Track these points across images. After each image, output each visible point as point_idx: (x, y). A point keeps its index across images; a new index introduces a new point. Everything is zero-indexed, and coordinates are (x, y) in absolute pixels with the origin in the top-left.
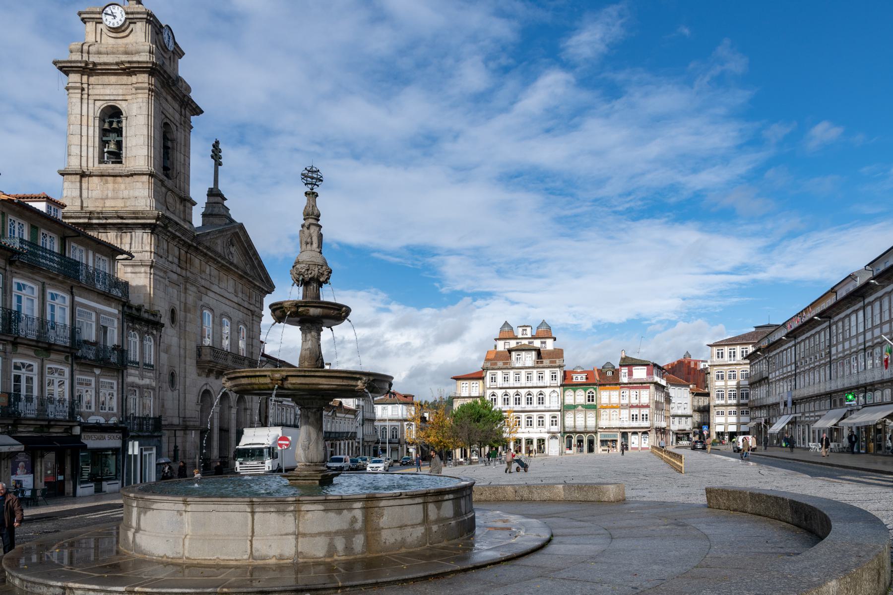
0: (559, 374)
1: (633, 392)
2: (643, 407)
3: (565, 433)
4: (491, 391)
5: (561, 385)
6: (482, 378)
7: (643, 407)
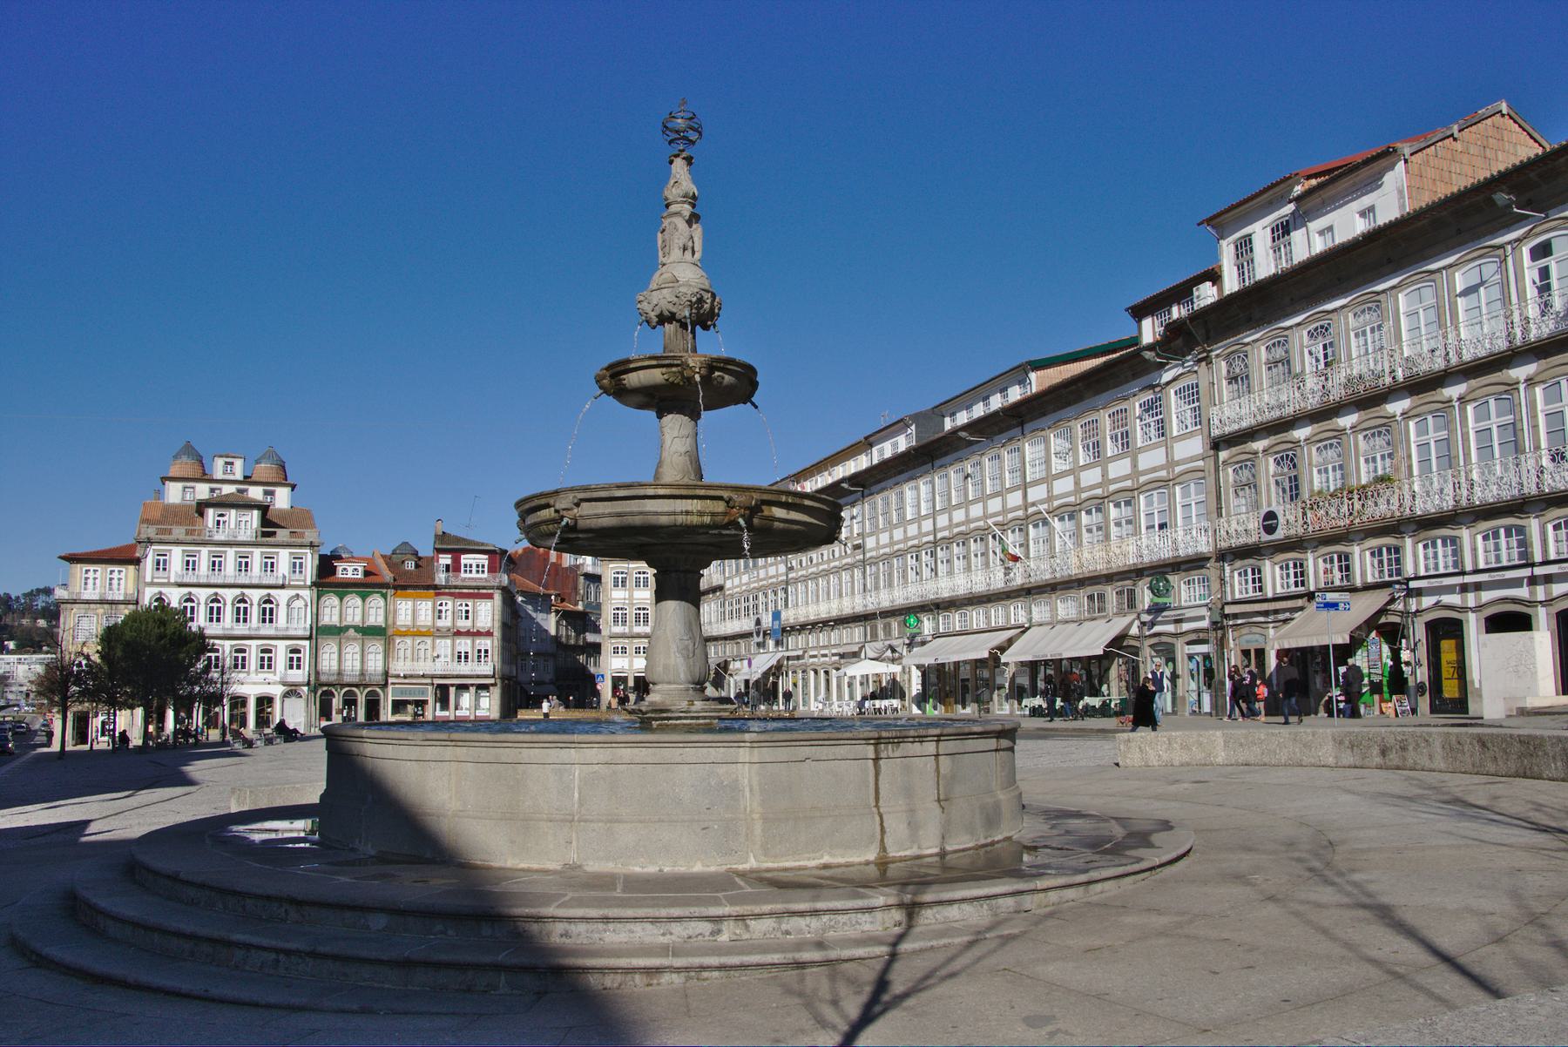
0: (310, 563)
2: (479, 634)
4: (156, 590)
5: (314, 584)
6: (137, 562)
7: (479, 634)
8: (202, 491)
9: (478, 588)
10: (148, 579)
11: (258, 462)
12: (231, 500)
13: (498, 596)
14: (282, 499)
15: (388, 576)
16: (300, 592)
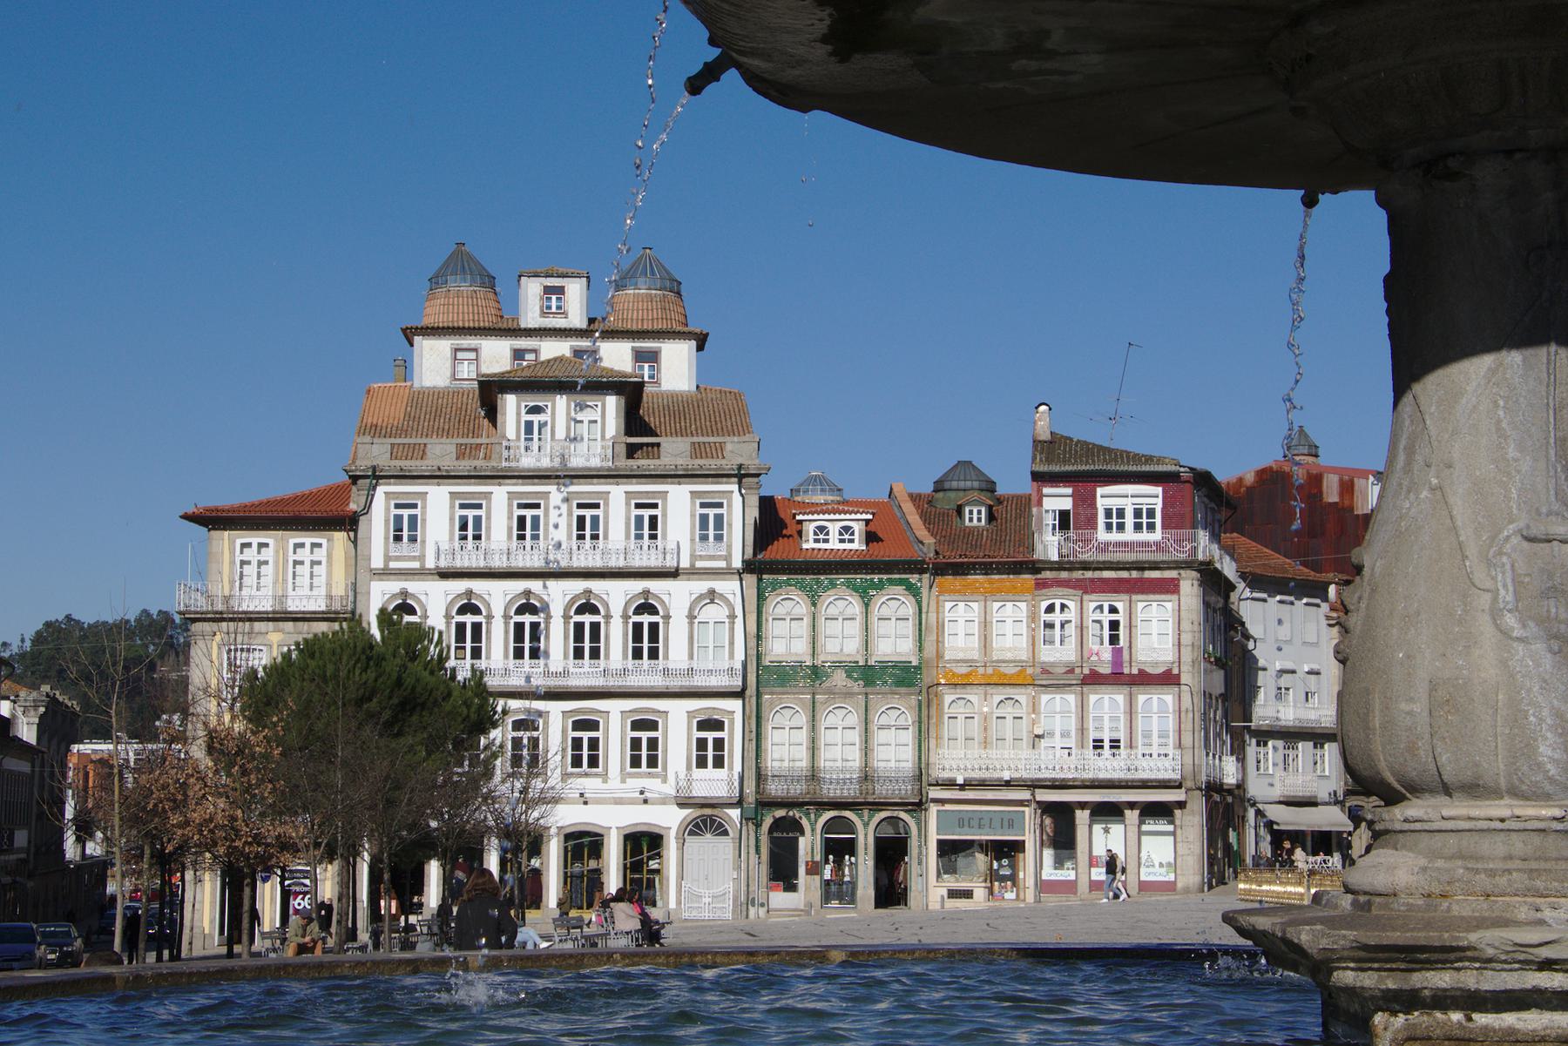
0: (739, 515)
1: (1095, 610)
3: (765, 804)
5: (750, 567)
6: (349, 523)
8: (496, 356)
9: (1140, 566)
10: (377, 562)
11: (619, 286)
12: (559, 373)
13: (1190, 587)
14: (677, 368)
15: (926, 543)
16: (722, 586)
